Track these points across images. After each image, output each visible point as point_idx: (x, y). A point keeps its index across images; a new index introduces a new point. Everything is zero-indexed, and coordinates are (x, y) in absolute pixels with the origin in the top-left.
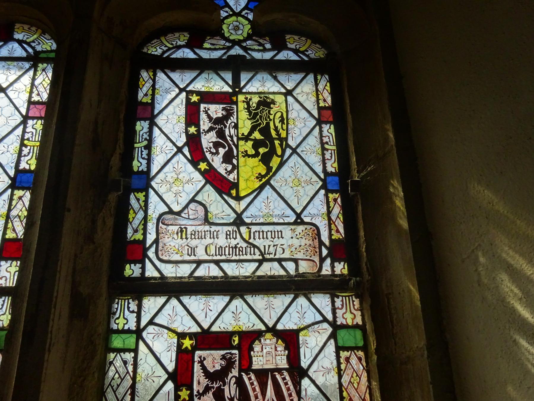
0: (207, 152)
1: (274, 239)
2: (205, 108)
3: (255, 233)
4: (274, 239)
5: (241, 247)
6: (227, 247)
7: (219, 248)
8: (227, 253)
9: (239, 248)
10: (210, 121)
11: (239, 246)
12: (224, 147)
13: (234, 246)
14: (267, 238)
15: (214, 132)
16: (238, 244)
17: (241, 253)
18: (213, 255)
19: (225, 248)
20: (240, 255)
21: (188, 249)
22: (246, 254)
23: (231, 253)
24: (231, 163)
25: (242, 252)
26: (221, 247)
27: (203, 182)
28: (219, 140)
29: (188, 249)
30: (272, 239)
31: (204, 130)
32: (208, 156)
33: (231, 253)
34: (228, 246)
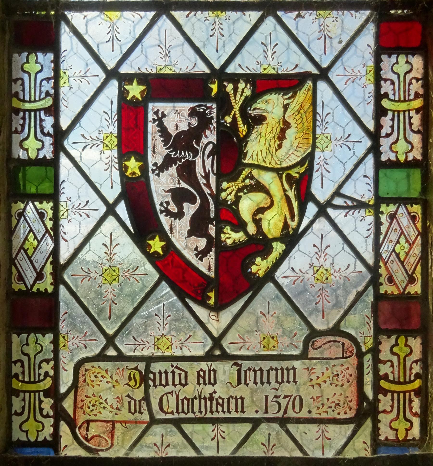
0: (162, 212)
1: (280, 384)
2: (156, 113)
3: (248, 372)
4: (280, 384)
5: (220, 397)
6: (195, 398)
7: (183, 400)
8: (196, 409)
9: (217, 400)
10: (166, 142)
11: (216, 396)
12: (193, 201)
13: (208, 396)
14: (269, 383)
15: (174, 167)
16: (215, 392)
17: (220, 408)
18: (172, 413)
19: (193, 400)
20: (218, 412)
21: (130, 403)
22: (229, 411)
23: (203, 409)
24: (207, 235)
25: (223, 406)
26: (185, 398)
27: (157, 276)
28: (184, 185)
29: (130, 403)
30: (277, 385)
31: (155, 164)
32: (164, 220)
33: (203, 409)
34: (197, 396)
